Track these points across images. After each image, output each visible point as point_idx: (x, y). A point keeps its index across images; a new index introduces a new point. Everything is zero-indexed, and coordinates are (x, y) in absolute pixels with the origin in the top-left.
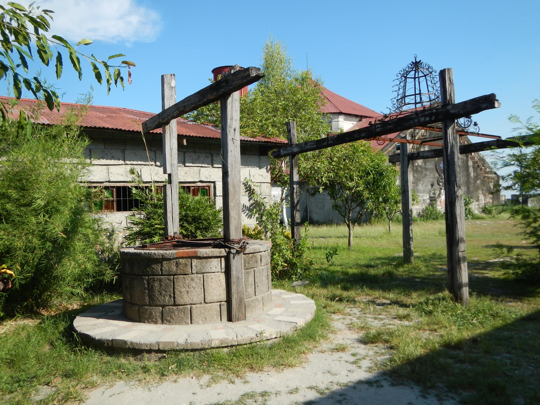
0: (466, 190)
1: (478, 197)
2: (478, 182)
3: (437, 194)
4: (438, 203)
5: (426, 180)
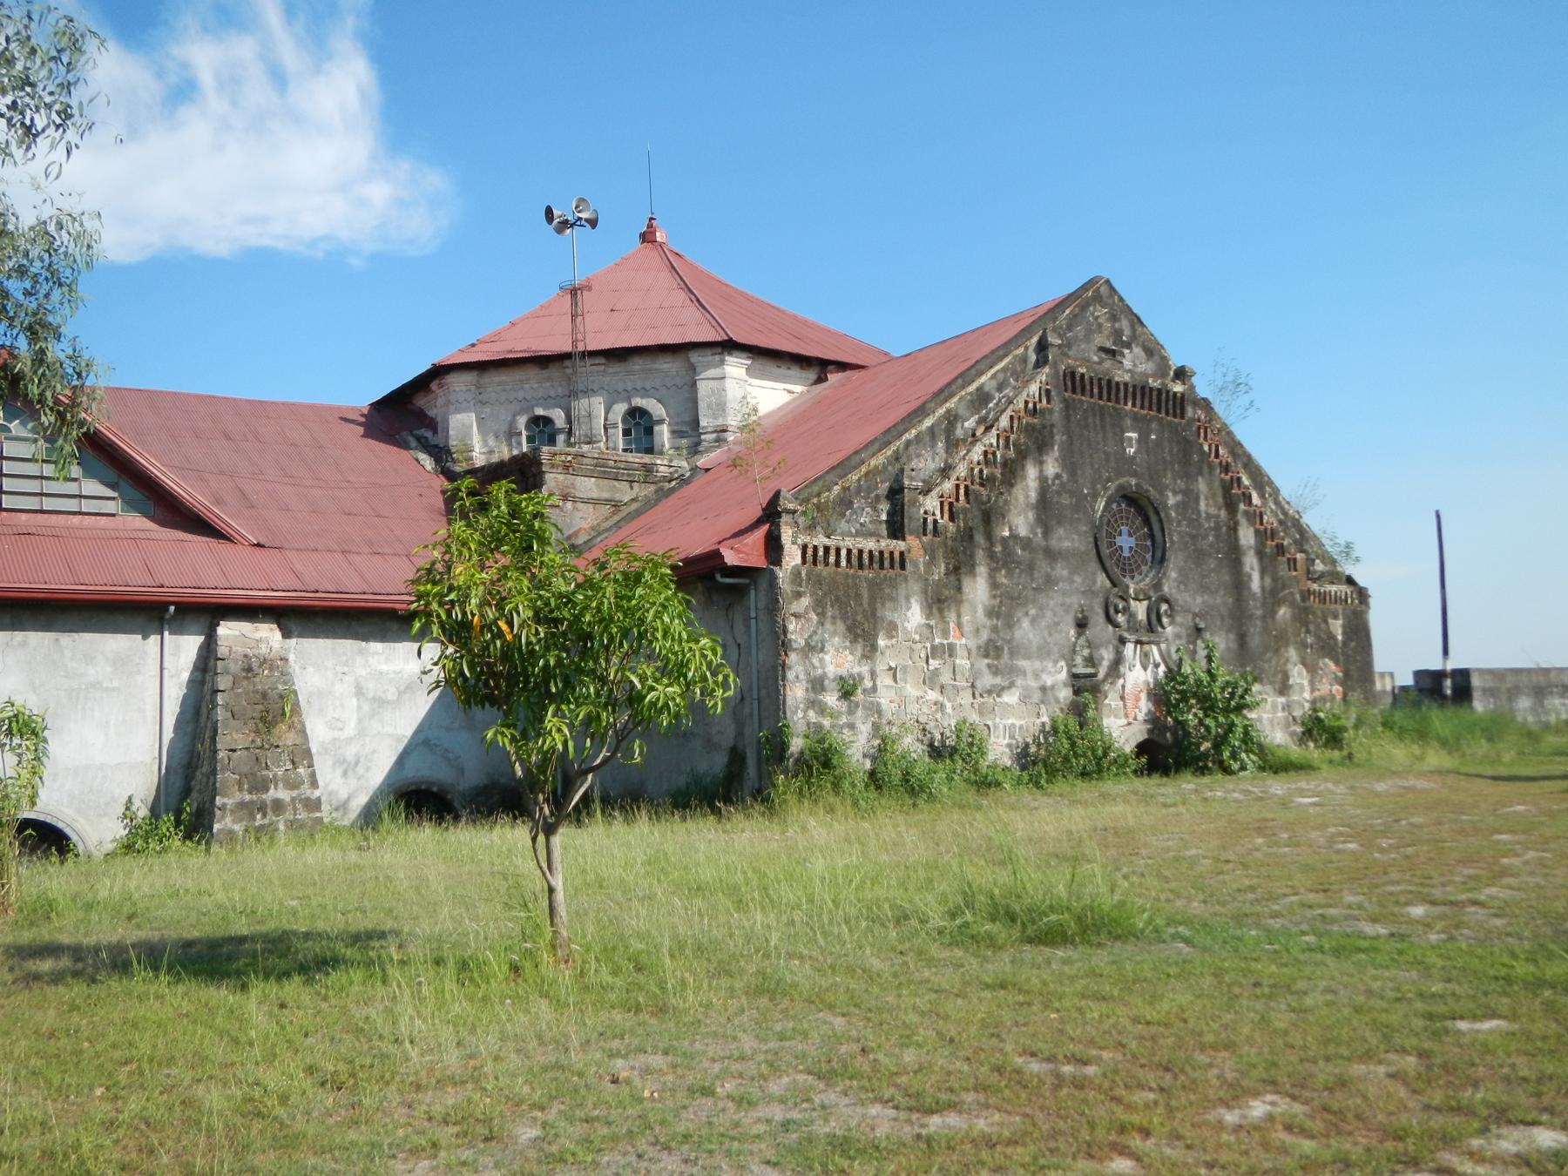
0: (1233, 645)
1: (1286, 676)
2: (1283, 612)
3: (1105, 663)
4: (1112, 700)
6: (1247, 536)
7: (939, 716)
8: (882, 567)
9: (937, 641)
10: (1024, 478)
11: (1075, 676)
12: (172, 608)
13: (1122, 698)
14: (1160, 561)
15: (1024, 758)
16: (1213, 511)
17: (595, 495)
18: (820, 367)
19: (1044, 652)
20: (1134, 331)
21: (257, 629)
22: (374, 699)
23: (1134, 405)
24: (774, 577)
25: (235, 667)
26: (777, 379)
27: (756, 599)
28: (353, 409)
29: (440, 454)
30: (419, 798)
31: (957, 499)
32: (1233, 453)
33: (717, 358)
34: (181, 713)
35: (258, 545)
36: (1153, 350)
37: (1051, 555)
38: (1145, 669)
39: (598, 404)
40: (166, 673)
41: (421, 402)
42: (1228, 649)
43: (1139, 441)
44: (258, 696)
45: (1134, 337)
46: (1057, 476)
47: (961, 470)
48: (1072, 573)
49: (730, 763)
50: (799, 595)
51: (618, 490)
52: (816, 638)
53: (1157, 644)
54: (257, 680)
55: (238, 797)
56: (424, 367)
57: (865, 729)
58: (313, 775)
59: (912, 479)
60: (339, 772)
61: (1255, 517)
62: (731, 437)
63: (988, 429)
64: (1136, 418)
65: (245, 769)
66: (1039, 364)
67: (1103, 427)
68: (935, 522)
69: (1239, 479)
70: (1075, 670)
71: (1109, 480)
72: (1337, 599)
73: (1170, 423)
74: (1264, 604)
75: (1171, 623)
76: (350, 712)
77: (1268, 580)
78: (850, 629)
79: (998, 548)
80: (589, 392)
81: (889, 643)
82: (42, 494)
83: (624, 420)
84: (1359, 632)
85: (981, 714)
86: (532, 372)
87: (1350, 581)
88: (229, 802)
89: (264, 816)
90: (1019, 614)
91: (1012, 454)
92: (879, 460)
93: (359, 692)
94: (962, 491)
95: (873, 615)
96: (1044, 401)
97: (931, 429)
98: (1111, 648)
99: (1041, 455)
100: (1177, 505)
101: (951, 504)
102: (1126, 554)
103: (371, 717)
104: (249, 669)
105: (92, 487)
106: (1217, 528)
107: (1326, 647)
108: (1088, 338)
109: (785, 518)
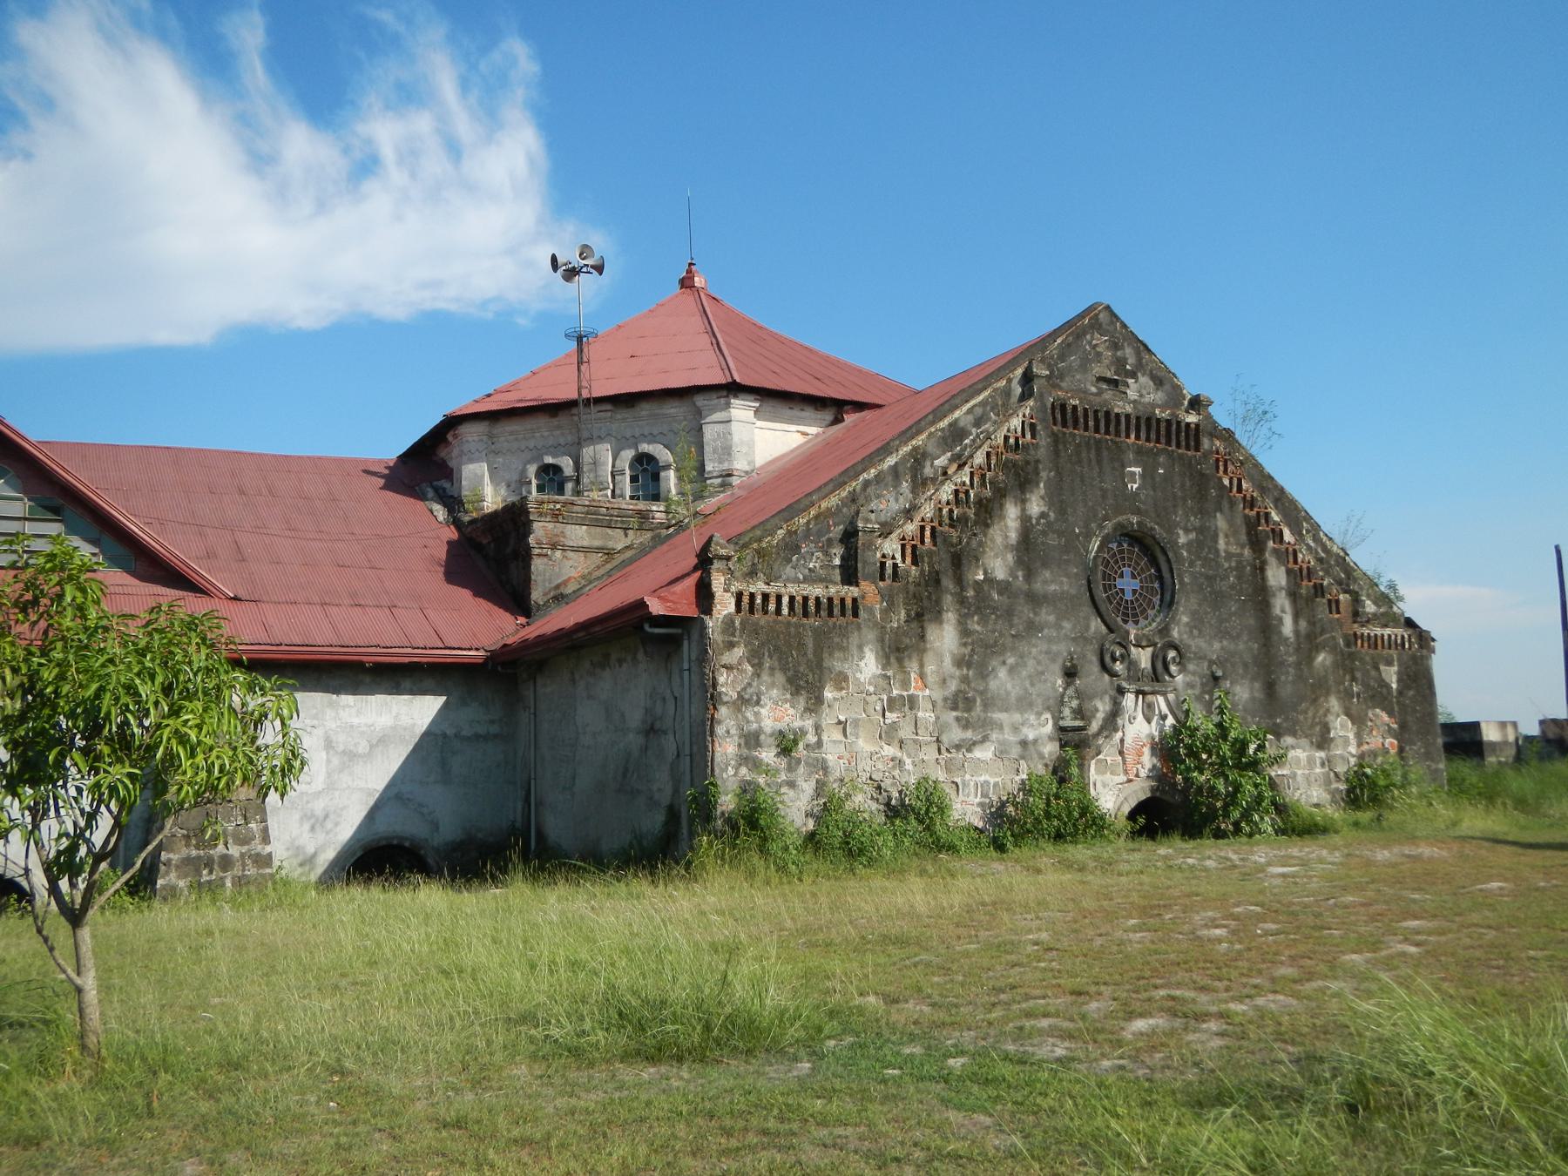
5: (1037, 649)
6: (1276, 576)
7: (896, 773)
8: (831, 614)
9: (895, 692)
10: (1002, 517)
11: (1063, 729)
13: (1121, 753)
14: (1168, 604)
15: (997, 815)
16: (1234, 549)
17: (585, 543)
18: (836, 408)
19: (1024, 703)
20: (1139, 359)
23: (1138, 437)
24: (704, 627)
26: (790, 421)
27: (688, 650)
28: (380, 461)
30: (378, 858)
31: (922, 542)
32: (1263, 490)
33: (723, 401)
35: (235, 599)
36: (1162, 378)
37: (1035, 600)
38: (1149, 721)
39: (605, 452)
41: (442, 453)
42: (1253, 699)
43: (1143, 476)
45: (1140, 366)
46: (1043, 515)
47: (927, 511)
48: (1060, 618)
49: (666, 823)
50: (731, 646)
51: (610, 538)
52: (750, 691)
53: (1164, 694)
55: (184, 852)
56: (437, 419)
57: (808, 787)
58: (265, 831)
59: (867, 520)
60: (307, 826)
61: (1287, 556)
62: (735, 481)
63: (961, 467)
64: (1139, 451)
66: (1023, 397)
67: (1099, 462)
68: (895, 566)
69: (1267, 515)
70: (1062, 723)
71: (1106, 518)
72: (1391, 643)
73: (1181, 457)
74: (1298, 649)
75: (1183, 670)
77: (1303, 624)
78: (790, 681)
79: (970, 593)
80: (593, 439)
81: (838, 695)
83: (631, 467)
84: (1419, 680)
85: (948, 770)
87: (1410, 623)
88: (174, 857)
89: (211, 872)
90: (994, 663)
91: (988, 493)
92: (833, 501)
93: (329, 745)
94: (928, 533)
95: (818, 666)
96: (1028, 436)
97: (895, 469)
98: (1107, 698)
99: (1023, 492)
100: (1189, 544)
101: (914, 547)
102: (1129, 596)
103: (341, 771)
106: (1239, 568)
107: (1378, 695)
108: (1084, 366)
109: (717, 565)
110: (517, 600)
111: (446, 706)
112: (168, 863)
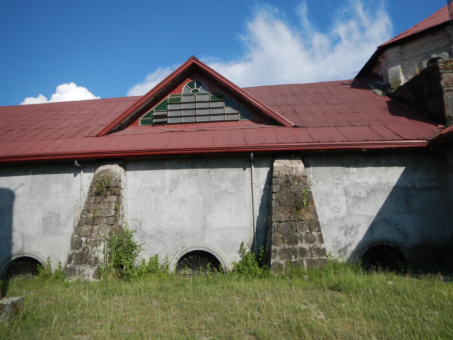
12: (252, 154)
21: (292, 163)
22: (354, 197)
25: (280, 181)
29: (385, 88)
34: (261, 204)
35: (295, 126)
40: (253, 185)
41: (375, 71)
44: (292, 195)
54: (292, 187)
58: (321, 236)
65: (286, 232)
76: (342, 203)
82: (210, 115)
86: (428, 40)
88: (278, 248)
89: (296, 257)
93: (346, 193)
103: (354, 206)
104: (288, 182)
105: (229, 110)
110: (437, 116)
111: (405, 172)
112: (275, 251)
